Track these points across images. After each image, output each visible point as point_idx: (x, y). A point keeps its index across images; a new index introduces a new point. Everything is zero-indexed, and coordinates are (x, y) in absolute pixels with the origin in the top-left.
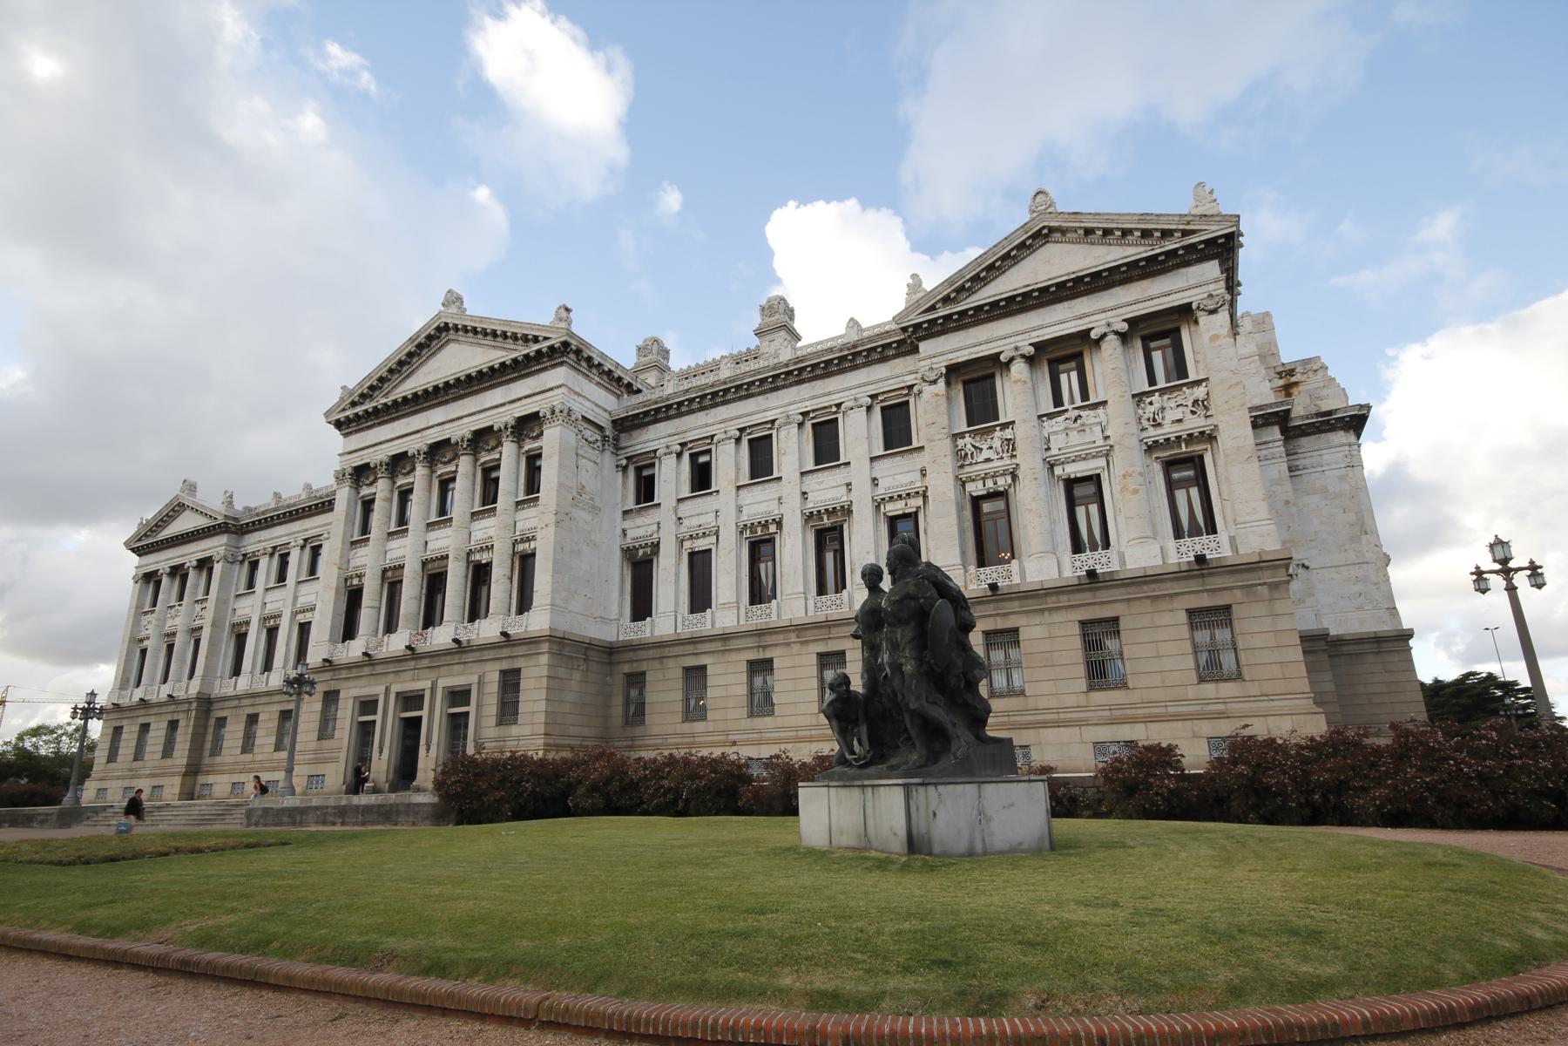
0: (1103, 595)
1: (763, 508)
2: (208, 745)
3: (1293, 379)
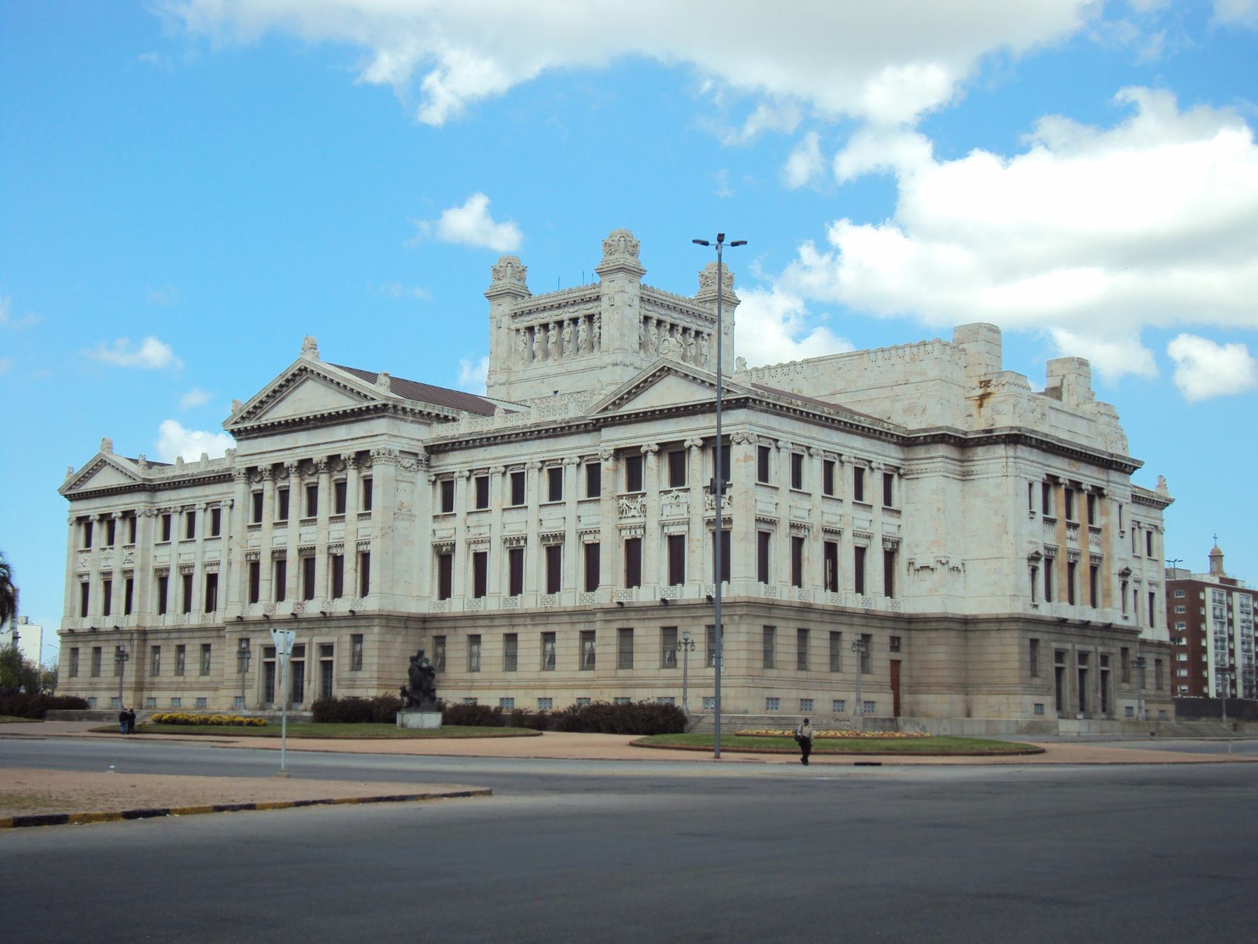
1: (516, 527)
2: (148, 668)
3: (989, 390)
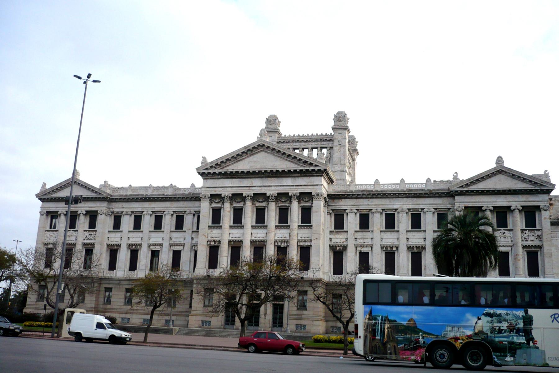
1: (391, 241)
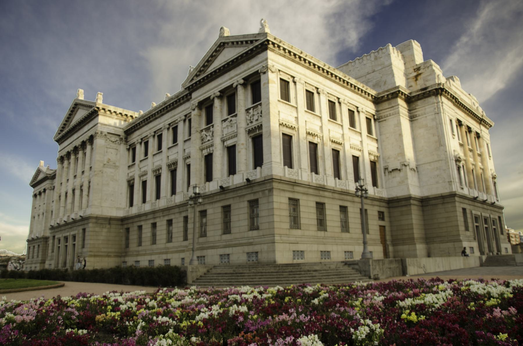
0: (228, 196)
3: (420, 72)
